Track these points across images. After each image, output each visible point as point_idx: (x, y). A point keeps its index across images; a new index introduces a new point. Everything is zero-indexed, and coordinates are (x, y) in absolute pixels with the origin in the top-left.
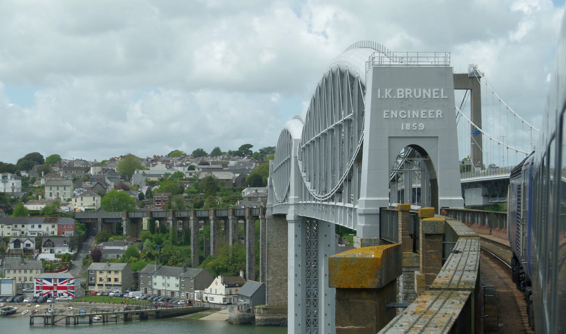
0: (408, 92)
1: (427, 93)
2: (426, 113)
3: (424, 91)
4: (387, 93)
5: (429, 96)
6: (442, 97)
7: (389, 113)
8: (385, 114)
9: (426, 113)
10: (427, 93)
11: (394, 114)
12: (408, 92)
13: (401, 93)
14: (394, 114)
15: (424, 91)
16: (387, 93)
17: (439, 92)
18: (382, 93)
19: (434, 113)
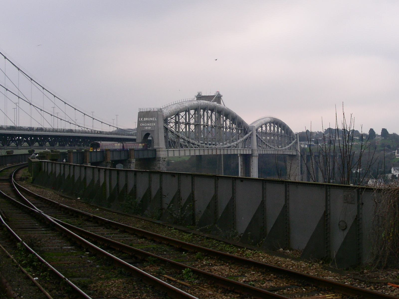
0: (147, 119)
1: (151, 119)
2: (151, 125)
3: (151, 118)
4: (141, 119)
5: (152, 120)
6: (155, 120)
7: (142, 125)
8: (141, 125)
9: (151, 125)
10: (151, 119)
11: (143, 125)
12: (147, 119)
13: (145, 119)
14: (143, 125)
15: (151, 118)
16: (141, 119)
17: (155, 119)
18: (140, 119)
19: (153, 124)
